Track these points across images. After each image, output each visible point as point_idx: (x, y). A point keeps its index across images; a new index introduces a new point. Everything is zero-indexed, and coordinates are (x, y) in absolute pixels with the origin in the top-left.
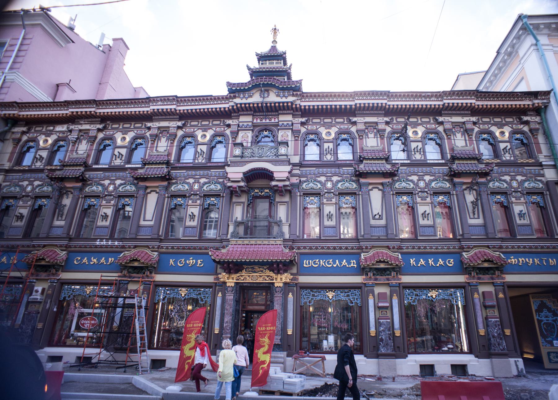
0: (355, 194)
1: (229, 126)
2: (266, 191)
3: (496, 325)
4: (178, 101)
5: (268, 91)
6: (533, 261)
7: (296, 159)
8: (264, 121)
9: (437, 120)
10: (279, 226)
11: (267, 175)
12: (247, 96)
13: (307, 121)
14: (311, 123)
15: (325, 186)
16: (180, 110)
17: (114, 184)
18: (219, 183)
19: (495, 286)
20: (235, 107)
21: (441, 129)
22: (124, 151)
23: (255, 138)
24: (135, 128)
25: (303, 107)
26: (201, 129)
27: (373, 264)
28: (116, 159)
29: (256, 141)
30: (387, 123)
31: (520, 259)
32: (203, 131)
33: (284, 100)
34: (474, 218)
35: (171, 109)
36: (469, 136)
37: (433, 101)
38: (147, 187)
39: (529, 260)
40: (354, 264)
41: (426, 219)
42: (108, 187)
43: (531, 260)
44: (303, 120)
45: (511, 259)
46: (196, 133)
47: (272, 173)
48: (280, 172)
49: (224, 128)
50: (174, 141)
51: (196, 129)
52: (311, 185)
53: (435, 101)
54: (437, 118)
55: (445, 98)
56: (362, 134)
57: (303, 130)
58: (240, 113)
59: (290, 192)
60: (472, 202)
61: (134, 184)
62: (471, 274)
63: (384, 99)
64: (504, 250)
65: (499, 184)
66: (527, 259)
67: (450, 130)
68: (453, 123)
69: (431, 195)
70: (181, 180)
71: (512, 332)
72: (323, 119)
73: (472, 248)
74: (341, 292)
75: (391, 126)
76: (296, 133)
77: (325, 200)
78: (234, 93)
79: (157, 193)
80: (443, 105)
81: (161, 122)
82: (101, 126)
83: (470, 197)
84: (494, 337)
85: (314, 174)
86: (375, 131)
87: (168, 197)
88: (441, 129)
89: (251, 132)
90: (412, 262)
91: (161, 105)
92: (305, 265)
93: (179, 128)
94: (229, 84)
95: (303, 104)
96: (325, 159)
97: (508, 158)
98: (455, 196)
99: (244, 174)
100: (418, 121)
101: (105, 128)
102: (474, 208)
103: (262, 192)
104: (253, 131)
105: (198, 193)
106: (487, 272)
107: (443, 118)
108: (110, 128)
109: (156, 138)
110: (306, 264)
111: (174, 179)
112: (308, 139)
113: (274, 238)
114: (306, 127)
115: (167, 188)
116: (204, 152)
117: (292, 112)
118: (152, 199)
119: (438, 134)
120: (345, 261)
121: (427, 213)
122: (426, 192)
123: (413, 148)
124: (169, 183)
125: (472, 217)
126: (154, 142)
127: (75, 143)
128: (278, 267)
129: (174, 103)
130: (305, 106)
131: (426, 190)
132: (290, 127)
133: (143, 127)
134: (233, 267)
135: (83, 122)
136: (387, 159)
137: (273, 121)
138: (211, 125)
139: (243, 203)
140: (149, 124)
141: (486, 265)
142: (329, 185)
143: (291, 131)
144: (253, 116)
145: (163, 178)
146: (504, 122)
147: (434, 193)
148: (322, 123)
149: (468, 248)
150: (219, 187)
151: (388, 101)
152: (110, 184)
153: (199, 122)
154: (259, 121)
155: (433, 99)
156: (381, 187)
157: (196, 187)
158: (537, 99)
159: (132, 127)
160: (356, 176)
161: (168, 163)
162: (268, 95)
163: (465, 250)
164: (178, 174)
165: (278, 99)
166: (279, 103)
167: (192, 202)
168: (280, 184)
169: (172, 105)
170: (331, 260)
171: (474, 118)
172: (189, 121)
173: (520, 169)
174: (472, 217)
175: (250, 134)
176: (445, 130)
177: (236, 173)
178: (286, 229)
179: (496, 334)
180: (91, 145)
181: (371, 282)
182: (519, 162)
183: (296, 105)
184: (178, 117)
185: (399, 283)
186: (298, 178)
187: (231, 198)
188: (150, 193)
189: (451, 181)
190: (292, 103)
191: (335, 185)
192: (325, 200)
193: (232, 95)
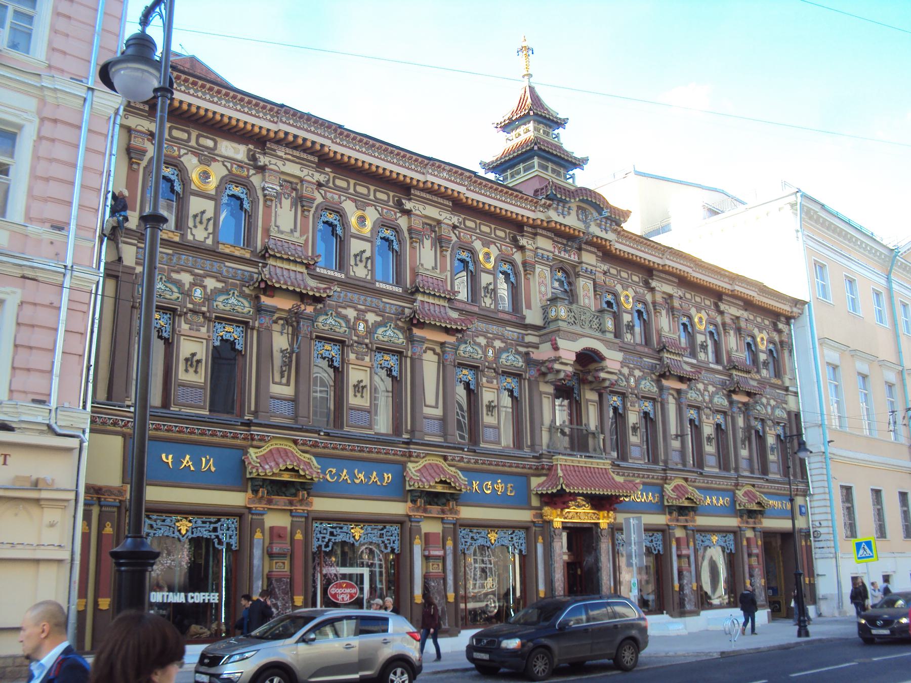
34: (280, 384)
36: (303, 211)
60: (282, 351)
106: (284, 489)
125: (277, 379)
141: (286, 477)
149: (260, 440)
163: (255, 443)
174: (277, 379)
185: (120, 501)
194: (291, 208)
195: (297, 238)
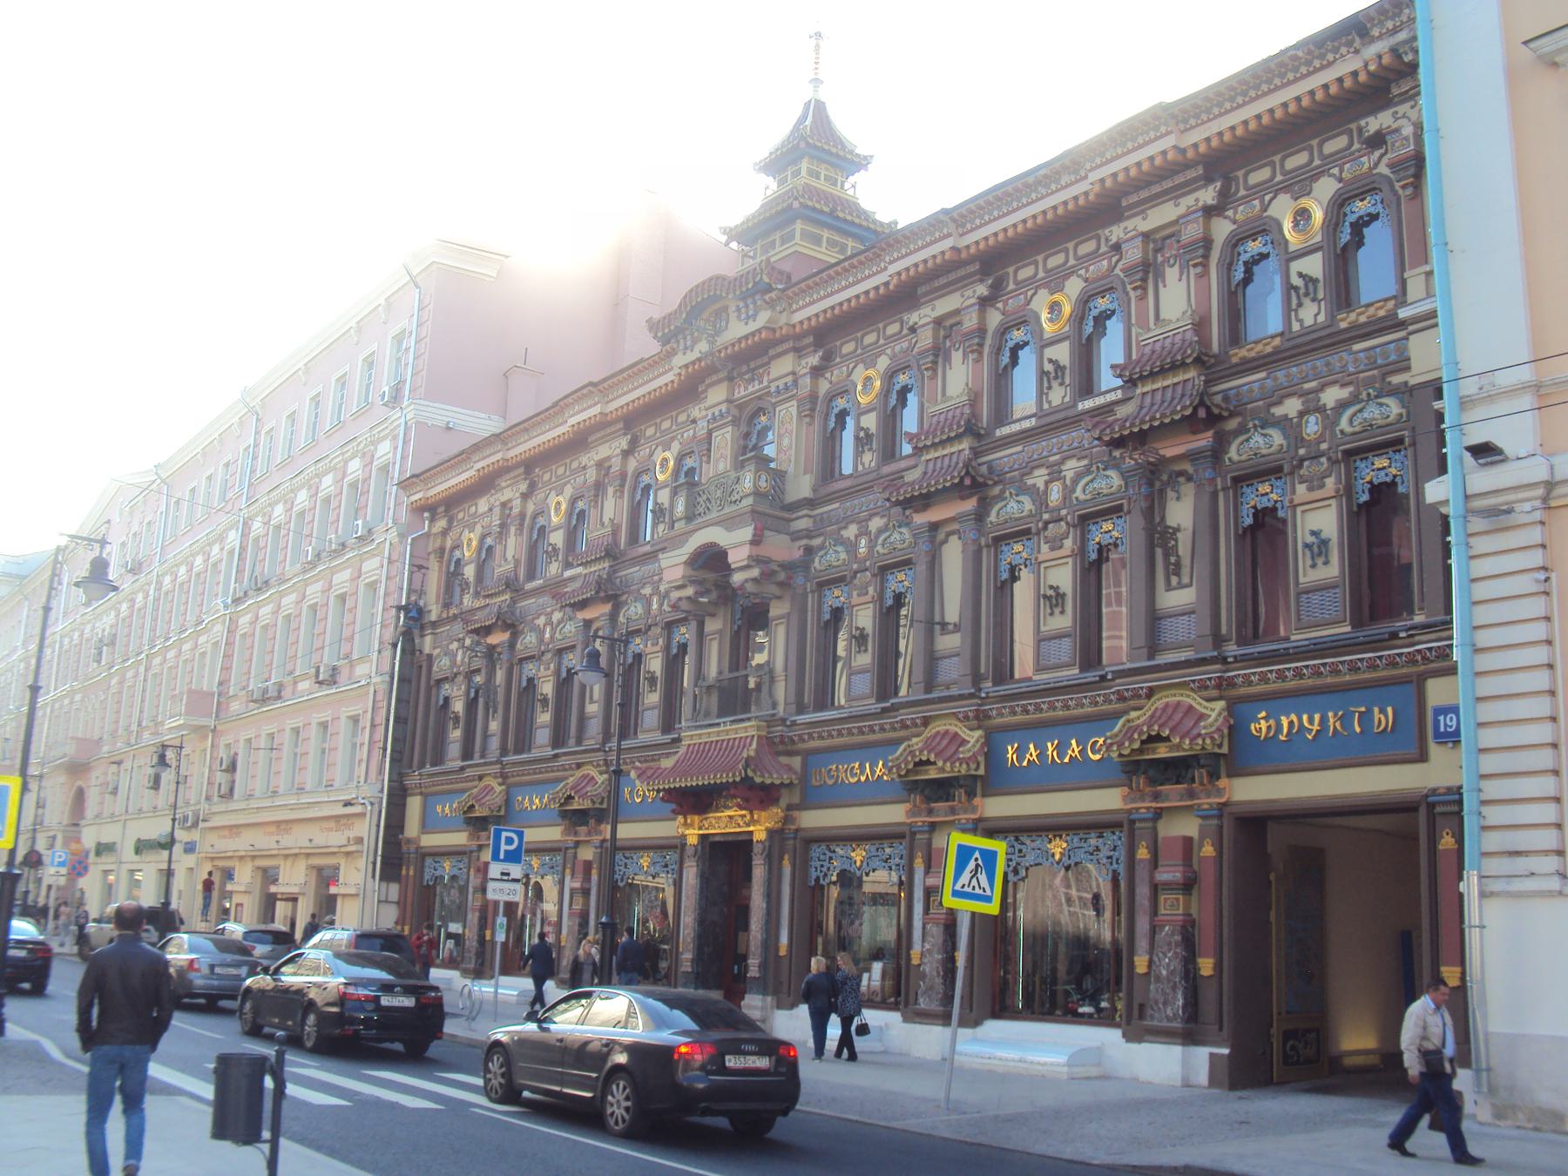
3: (1169, 944)
6: (1323, 720)
13: (822, 358)
31: (1285, 722)
33: (753, 326)
39: (1311, 721)
43: (1317, 717)
64: (1243, 691)
66: (1305, 717)
68: (1146, 236)
71: (1218, 966)
84: (1158, 979)
97: (1309, 321)
104: (735, 422)
107: (1123, 225)
130: (801, 322)
143: (794, 403)
158: (1373, 40)
171: (1211, 188)
173: (1335, 361)
177: (673, 566)
179: (1164, 972)
182: (1343, 325)
186: (804, 542)
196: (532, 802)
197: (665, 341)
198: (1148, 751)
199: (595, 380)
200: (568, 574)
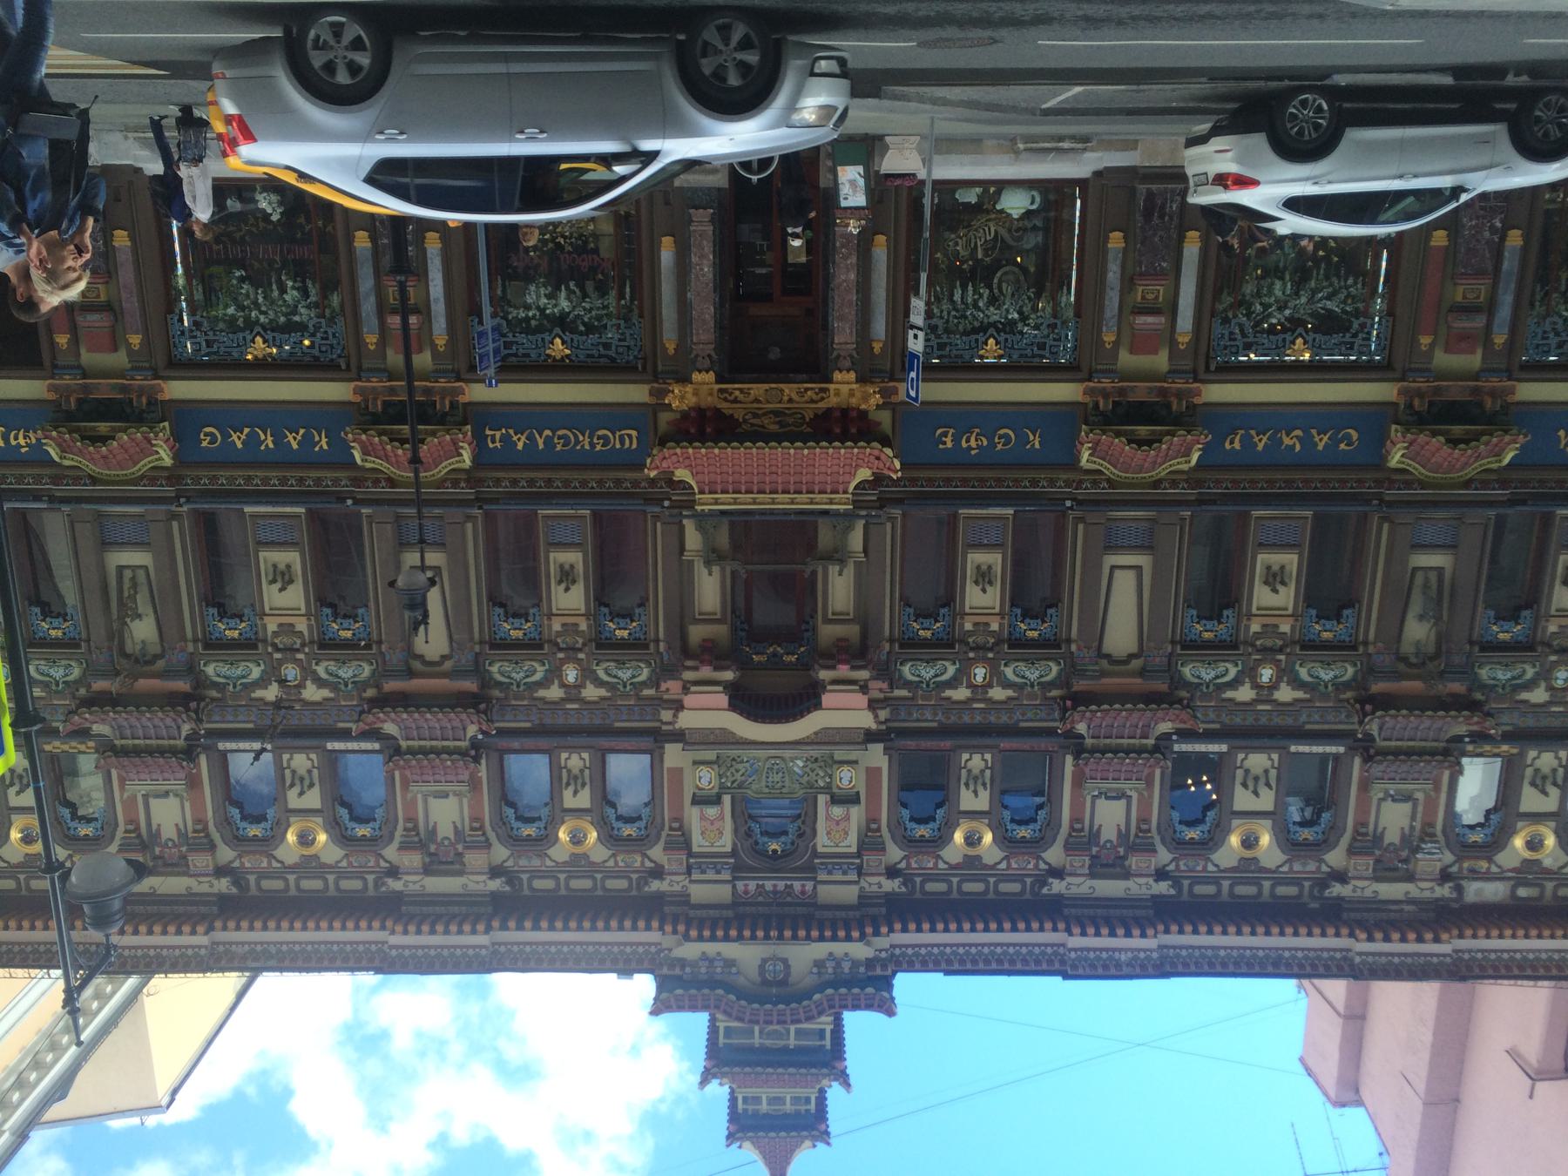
0: (493, 646)
1: (892, 872)
2: (763, 658)
4: (1063, 962)
5: (765, 983)
7: (673, 755)
8: (781, 885)
9: (236, 883)
10: (714, 551)
11: (746, 701)
12: (830, 965)
14: (634, 876)
15: (583, 670)
16: (1055, 929)
17: (1257, 686)
18: (907, 684)
19: (79, 367)
20: (869, 930)
21: (226, 854)
22: (1243, 799)
23: (808, 831)
24: (1216, 881)
25: (655, 924)
26: (986, 867)
27: (433, 434)
28: (1266, 771)
29: (805, 818)
30: (394, 872)
32: (978, 858)
33: (711, 948)
34: (134, 568)
35: (1084, 934)
36: (137, 829)
37: (243, 944)
38: (1142, 673)
40: (493, 437)
41: (282, 567)
42: (1279, 679)
44: (655, 885)
45: (28, 445)
46: (998, 854)
47: (733, 707)
48: (708, 710)
49: (908, 864)
50: (1072, 828)
51: (1003, 865)
52: (625, 675)
53: (237, 943)
54: (234, 890)
55: (203, 952)
56: (471, 837)
57: (657, 853)
58: (857, 914)
59: (686, 652)
60: (139, 616)
61: (1187, 685)
62: (149, 403)
63: (397, 947)
64: (48, 471)
65: (52, 672)
67: (195, 847)
68: (186, 874)
69: (265, 641)
70: (1032, 696)
72: (595, 888)
73: (142, 477)
74: (527, 355)
75: (383, 864)
76: (681, 842)
77: (583, 626)
78: (870, 978)
79: (1108, 656)
80: (211, 929)
81: (1121, 894)
82: (1337, 889)
83: (143, 630)
85: (617, 707)
86: (433, 848)
87: (1069, 641)
88: (226, 854)
89: (820, 849)
90: (324, 440)
91: (1120, 950)
92: (634, 433)
93: (1058, 873)
94: (888, 1008)
95: (654, 936)
96: (585, 755)
98: (189, 634)
99: (818, 706)
100: (297, 881)
101: (1323, 883)
102: (133, 598)
103: (775, 655)
104: (815, 854)
105: (971, 655)
107: (215, 890)
108: (1307, 884)
109: (1135, 841)
110: (630, 436)
111: (1054, 698)
112: (642, 824)
113: (723, 513)
114: (648, 864)
115: (1072, 669)
116: (967, 785)
117: (692, 913)
118: (1121, 634)
119: (236, 837)
120: (520, 446)
121: (278, 585)
122: (278, 650)
123: (316, 790)
124: (1068, 685)
126: (1139, 829)
127: (1427, 834)
128: (707, 427)
129: (1073, 955)
131: (277, 656)
132: (696, 864)
133: (1186, 883)
134: (844, 426)
135: (1407, 908)
136: (393, 751)
137: (752, 885)
138: (955, 880)
139: (828, 621)
140: (1163, 888)
141: (103, 427)
142: (571, 675)
143: (695, 849)
144: (815, 905)
145: (1081, 700)
146: (22, 877)
147: (255, 647)
148: (599, 876)
150: (906, 670)
151: (384, 943)
152: (1274, 686)
153: (996, 892)
154: (797, 885)
155: (240, 950)
156: (417, 665)
157: (980, 673)
159: (1226, 884)
160: (488, 700)
161: (1079, 751)
162: (762, 967)
164: (1043, 715)
165: (730, 950)
166: (726, 938)
167: (987, 624)
168: (706, 672)
169: (1081, 949)
170: (559, 448)
172: (1028, 896)
174: (141, 573)
175: (823, 842)
176: (212, 847)
177: (844, 710)
178: (693, 539)
180: (1365, 824)
181: (442, 384)
183: (675, 932)
184: (1066, 911)
185: (359, 379)
187: (864, 635)
188: (1132, 656)
189: (201, 682)
190: (687, 938)
191: (554, 674)
192: (583, 626)
193: (879, 972)
194: (158, 830)
195: (138, 788)
196: (1306, 441)
197: (887, 984)
198: (113, 429)
199: (1059, 979)
200: (1224, 748)
